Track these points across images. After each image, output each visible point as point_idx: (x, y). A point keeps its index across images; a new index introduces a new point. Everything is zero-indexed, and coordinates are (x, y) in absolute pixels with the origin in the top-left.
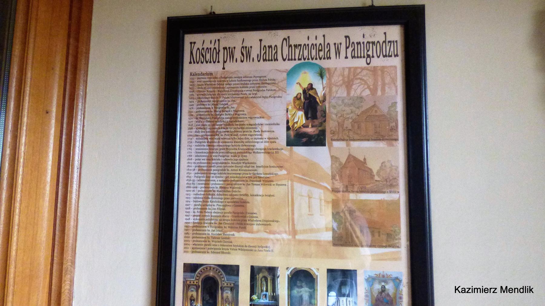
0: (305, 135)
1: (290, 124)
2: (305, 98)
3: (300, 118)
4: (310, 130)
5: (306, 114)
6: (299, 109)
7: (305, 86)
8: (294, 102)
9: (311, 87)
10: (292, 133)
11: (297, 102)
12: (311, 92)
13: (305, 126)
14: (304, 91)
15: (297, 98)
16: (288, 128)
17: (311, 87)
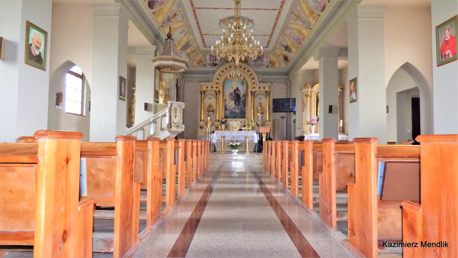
0: (235, 113)
1: (228, 107)
2: (235, 95)
3: (231, 104)
4: (237, 111)
5: (235, 103)
6: (232, 100)
7: (235, 88)
8: (230, 96)
9: (237, 89)
10: (228, 112)
11: (231, 96)
12: (238, 92)
13: (235, 109)
14: (235, 91)
15: (231, 94)
16: (226, 109)
17: (237, 89)
